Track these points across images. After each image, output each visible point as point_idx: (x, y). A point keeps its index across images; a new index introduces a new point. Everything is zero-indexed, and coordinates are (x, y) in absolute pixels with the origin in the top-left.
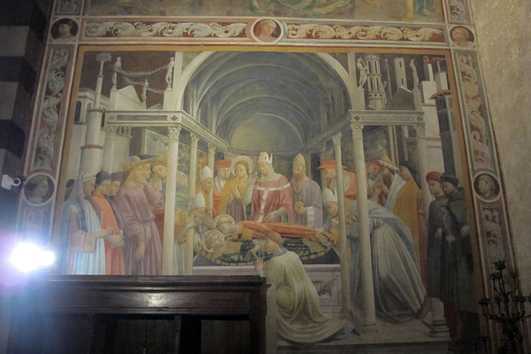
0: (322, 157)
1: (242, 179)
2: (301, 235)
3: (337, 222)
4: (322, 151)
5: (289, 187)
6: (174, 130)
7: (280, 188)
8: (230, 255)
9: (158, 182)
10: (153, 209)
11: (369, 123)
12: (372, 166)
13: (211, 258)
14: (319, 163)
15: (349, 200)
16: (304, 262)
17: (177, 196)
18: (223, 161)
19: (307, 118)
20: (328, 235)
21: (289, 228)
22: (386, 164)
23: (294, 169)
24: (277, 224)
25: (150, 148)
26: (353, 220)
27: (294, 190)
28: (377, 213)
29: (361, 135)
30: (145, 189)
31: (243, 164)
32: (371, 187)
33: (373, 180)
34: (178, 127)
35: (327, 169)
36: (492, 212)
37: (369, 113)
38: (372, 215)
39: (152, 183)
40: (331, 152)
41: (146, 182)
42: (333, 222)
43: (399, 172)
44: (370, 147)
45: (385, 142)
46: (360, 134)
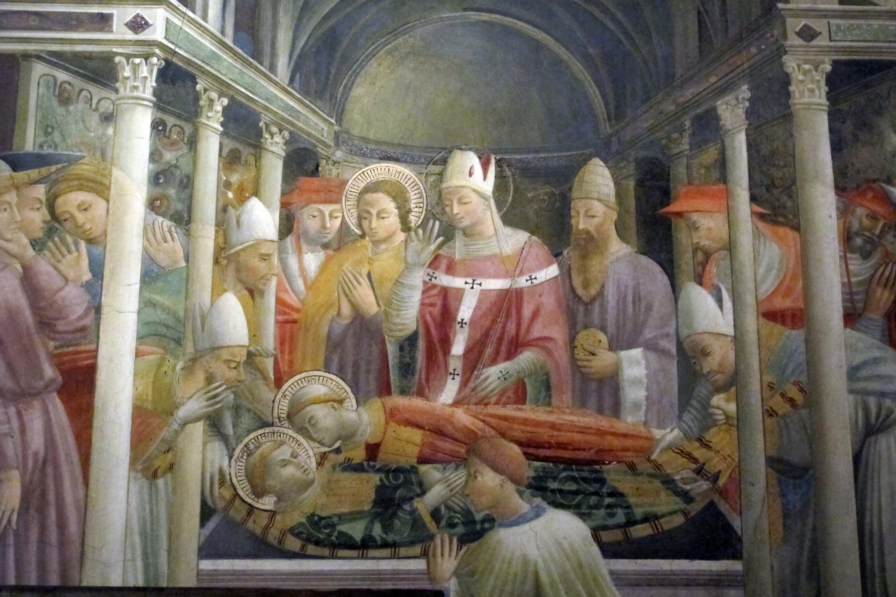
0: (679, 171)
1: (383, 246)
2: (600, 451)
3: (732, 407)
4: (676, 151)
5: (555, 277)
6: (135, 68)
7: (522, 282)
8: (335, 519)
9: (75, 254)
10: (56, 348)
11: (851, 50)
12: (863, 206)
13: (267, 528)
14: (666, 196)
15: (777, 328)
16: (609, 551)
17: (146, 304)
18: (315, 182)
19: (626, 34)
20: (699, 453)
21: (553, 426)
23: (573, 213)
24: (510, 411)
25: (47, 130)
26: (792, 401)
27: (573, 290)
28: (879, 377)
29: (824, 94)
30: (28, 280)
31: (388, 194)
32: (860, 283)
33: (866, 256)
34: (154, 55)
35: (695, 217)
37: (853, 17)
38: (861, 385)
39: (53, 255)
40: (710, 155)
41: (31, 252)
42: (718, 408)
44: (856, 138)
46: (817, 90)
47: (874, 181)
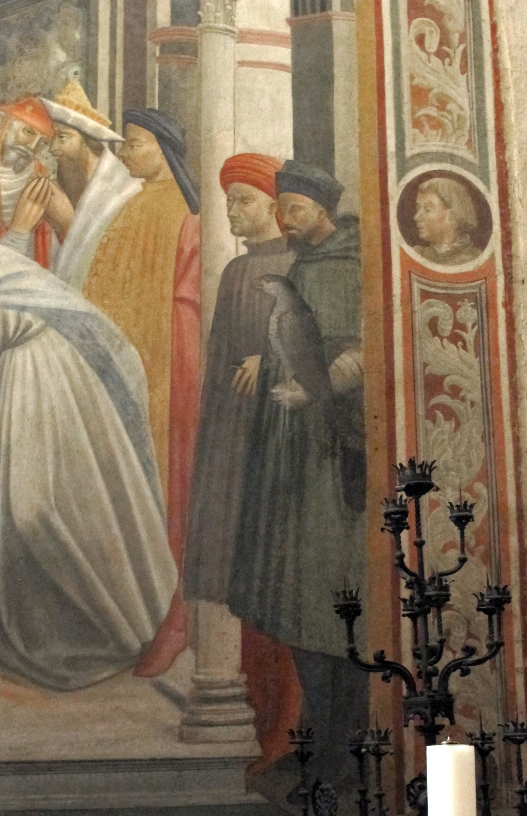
12: (21, 120)
22: (73, 116)
28: (21, 291)
32: (9, 197)
33: (19, 170)
36: (455, 308)
43: (117, 145)
44: (21, 52)
45: (78, 36)
47: (35, 96)
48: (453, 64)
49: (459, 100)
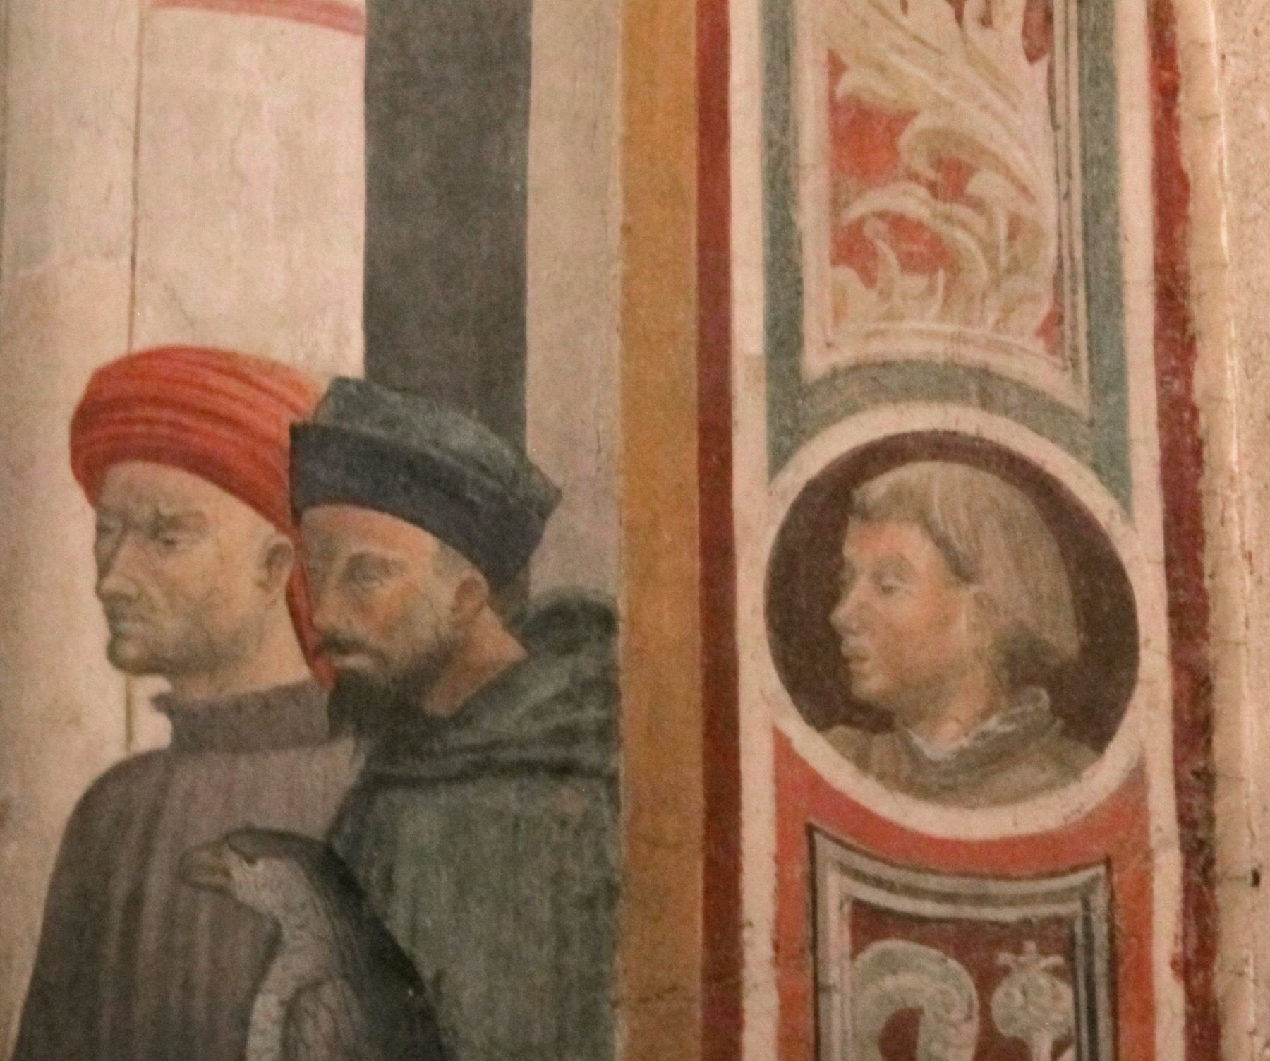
36: (987, 979)
48: (998, 21)
49: (1016, 157)
